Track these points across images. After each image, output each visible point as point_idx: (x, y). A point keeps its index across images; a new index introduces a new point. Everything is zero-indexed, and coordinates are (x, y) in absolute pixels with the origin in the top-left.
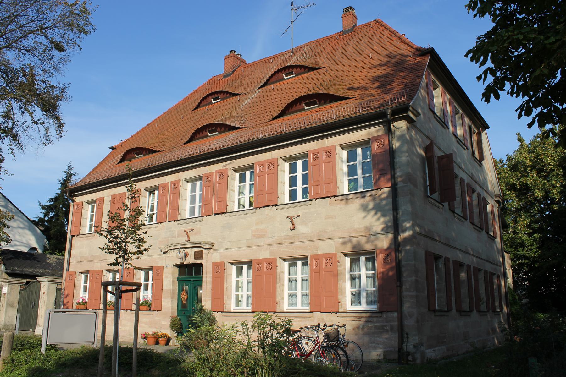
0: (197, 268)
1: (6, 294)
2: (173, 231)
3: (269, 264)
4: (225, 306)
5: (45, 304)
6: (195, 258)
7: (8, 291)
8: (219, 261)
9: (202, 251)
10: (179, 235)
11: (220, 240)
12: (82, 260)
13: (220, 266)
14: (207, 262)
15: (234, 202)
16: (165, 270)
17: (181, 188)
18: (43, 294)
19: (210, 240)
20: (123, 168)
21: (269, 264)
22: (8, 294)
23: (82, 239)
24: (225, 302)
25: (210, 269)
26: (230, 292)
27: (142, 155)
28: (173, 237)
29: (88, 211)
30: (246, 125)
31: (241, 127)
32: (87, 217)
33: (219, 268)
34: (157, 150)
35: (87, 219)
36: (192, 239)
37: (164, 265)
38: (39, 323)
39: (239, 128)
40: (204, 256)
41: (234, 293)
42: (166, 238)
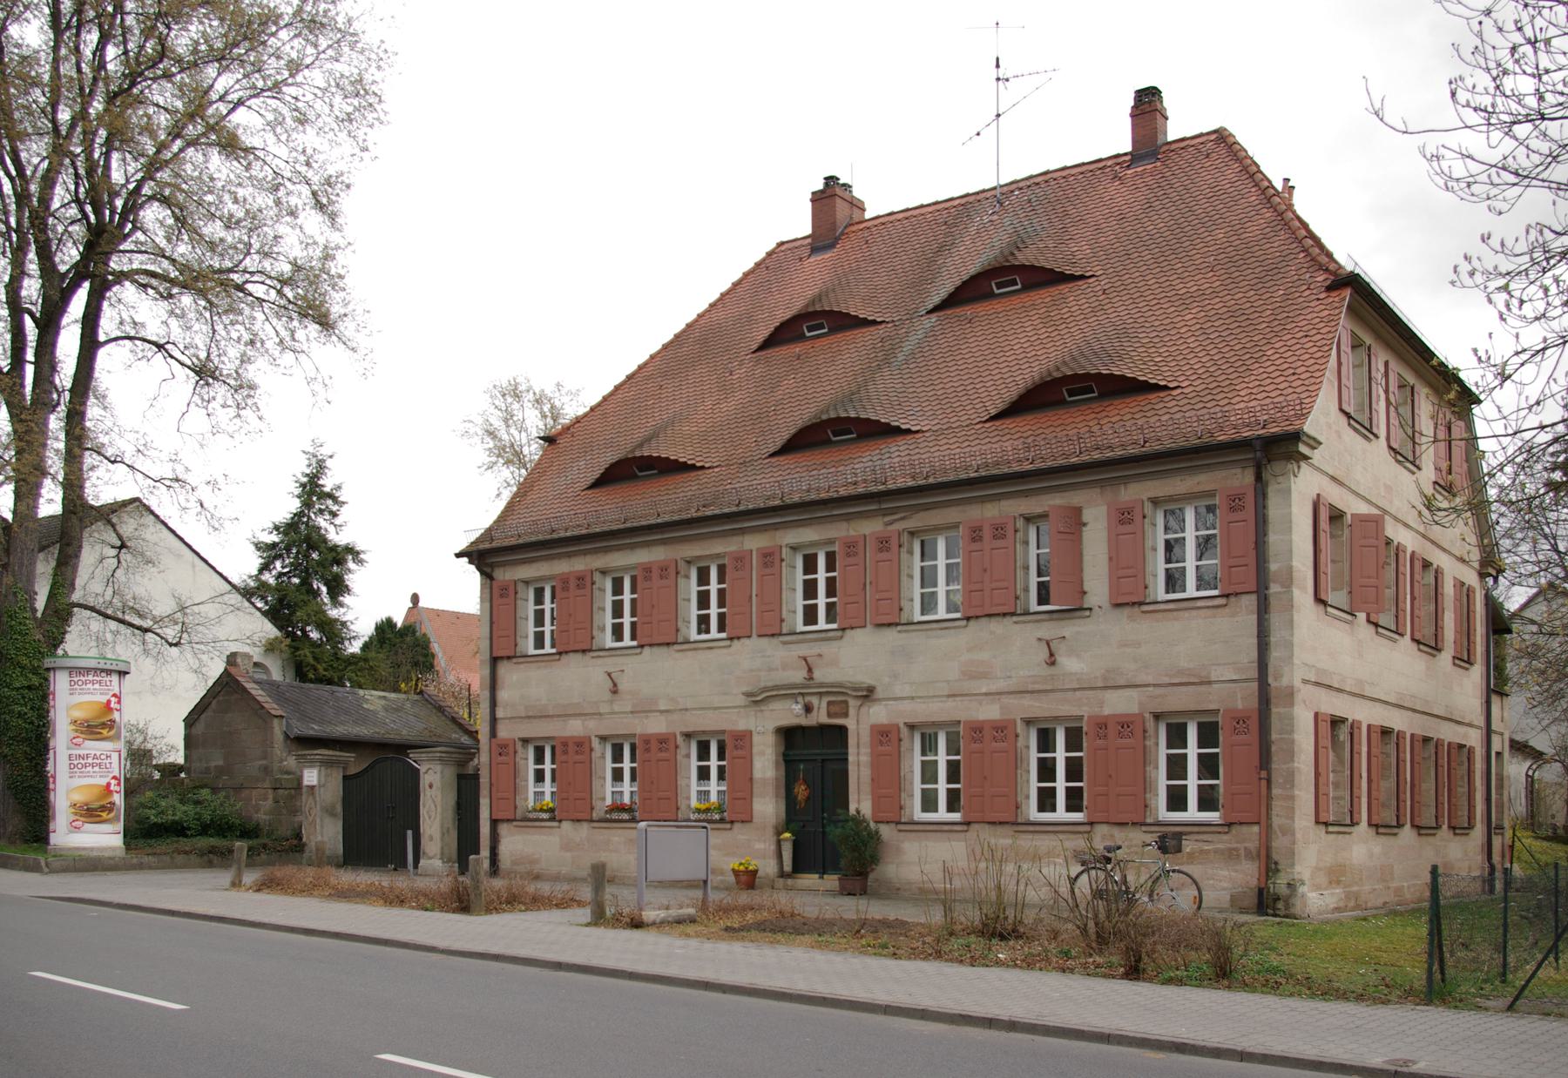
0: (836, 736)
1: (317, 788)
2: (769, 657)
3: (1241, 722)
4: (903, 812)
5: (439, 809)
6: (829, 715)
7: (319, 781)
8: (885, 721)
9: (846, 702)
10: (785, 667)
11: (887, 680)
12: (531, 714)
13: (890, 732)
14: (860, 724)
15: (912, 600)
16: (756, 739)
17: (784, 564)
18: (427, 787)
19: (866, 680)
20: (614, 508)
21: (1241, 722)
22: (320, 787)
23: (522, 666)
24: (902, 802)
25: (866, 737)
26: (912, 783)
27: (655, 472)
28: (770, 670)
29: (527, 600)
30: (923, 425)
31: (914, 429)
32: (604, 626)
33: (885, 736)
34: (698, 464)
35: (527, 619)
36: (817, 674)
37: (753, 729)
38: (427, 851)
39: (909, 431)
40: (852, 711)
41: (918, 787)
42: (752, 671)
